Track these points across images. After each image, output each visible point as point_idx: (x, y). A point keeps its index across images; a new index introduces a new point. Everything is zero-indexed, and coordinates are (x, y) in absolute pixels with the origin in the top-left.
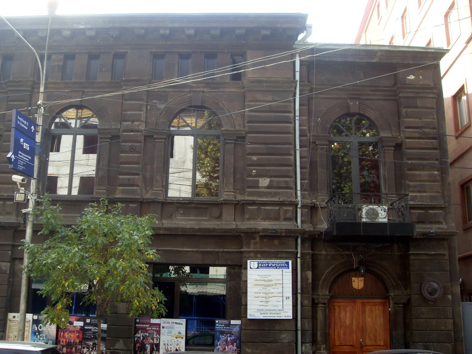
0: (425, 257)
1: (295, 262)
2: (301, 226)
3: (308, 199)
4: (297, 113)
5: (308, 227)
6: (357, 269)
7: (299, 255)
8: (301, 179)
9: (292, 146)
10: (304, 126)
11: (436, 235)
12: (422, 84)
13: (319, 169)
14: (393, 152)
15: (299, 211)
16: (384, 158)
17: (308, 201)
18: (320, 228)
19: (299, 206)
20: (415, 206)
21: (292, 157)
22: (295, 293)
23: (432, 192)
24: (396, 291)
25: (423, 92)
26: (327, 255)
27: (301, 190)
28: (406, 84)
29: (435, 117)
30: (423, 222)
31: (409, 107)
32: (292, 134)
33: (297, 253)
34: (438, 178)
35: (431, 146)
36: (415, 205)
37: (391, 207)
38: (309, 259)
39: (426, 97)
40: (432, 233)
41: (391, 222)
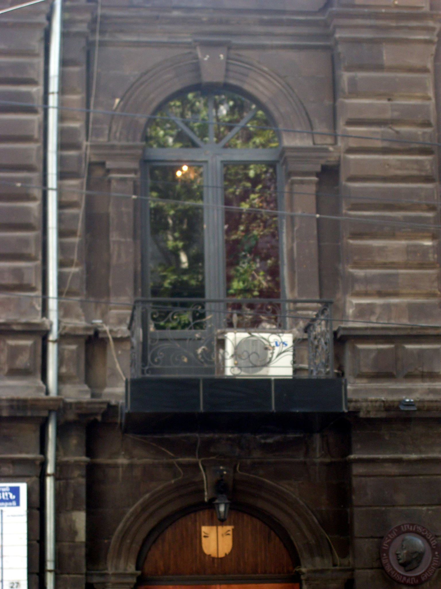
0: (394, 470)
1: (37, 488)
2: (59, 392)
3: (78, 317)
4: (54, 86)
5: (77, 393)
6: (211, 505)
7: (50, 469)
8: (61, 264)
9: (36, 176)
10: (74, 119)
11: (419, 409)
12: (397, 7)
13: (114, 237)
14: (313, 189)
15: (52, 350)
16: (291, 206)
17: (78, 323)
18: (112, 395)
19: (53, 336)
20: (368, 333)
21: (34, 206)
22: (37, 569)
23: (415, 295)
24: (317, 559)
25: (398, 28)
26: (131, 466)
27: (60, 293)
28: (354, 6)
29: (431, 94)
30: (389, 376)
31: (361, 68)
32: (36, 141)
33: (44, 464)
34: (432, 257)
35: (415, 173)
36: (366, 329)
37: (306, 336)
38: (78, 479)
39: (407, 41)
40: (409, 404)
41: (304, 375)
